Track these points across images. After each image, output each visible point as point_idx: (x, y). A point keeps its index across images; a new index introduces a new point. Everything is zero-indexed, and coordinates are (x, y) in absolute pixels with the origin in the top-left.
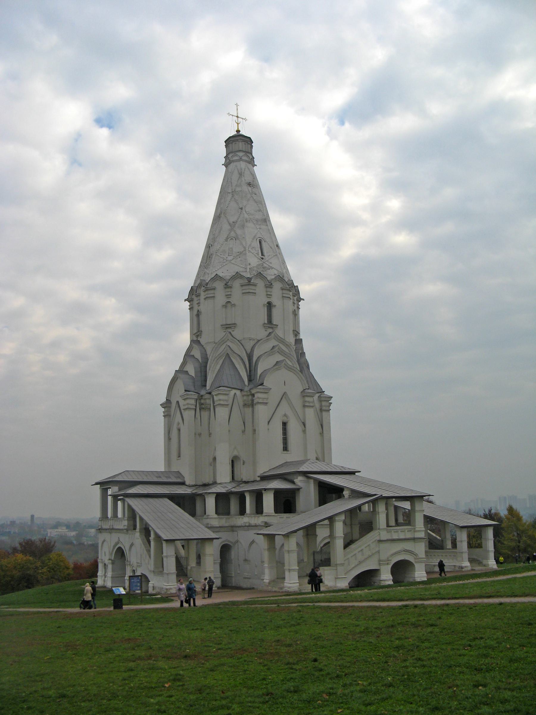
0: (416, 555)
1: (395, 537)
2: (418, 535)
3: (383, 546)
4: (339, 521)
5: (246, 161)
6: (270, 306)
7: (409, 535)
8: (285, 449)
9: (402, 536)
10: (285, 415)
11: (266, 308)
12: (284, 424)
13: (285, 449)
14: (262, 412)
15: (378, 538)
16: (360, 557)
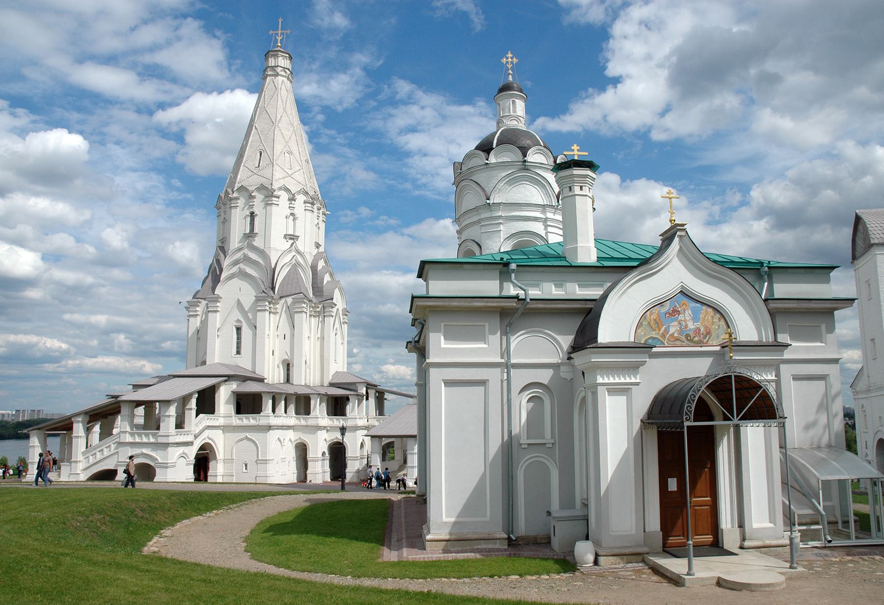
0: (156, 459)
1: (138, 440)
2: (161, 440)
3: (121, 449)
4: (78, 422)
5: (272, 75)
6: (252, 215)
7: (152, 440)
8: (238, 352)
9: (145, 440)
10: (238, 321)
11: (249, 219)
12: (239, 329)
13: (238, 352)
14: (216, 320)
15: (118, 440)
16: (99, 456)
